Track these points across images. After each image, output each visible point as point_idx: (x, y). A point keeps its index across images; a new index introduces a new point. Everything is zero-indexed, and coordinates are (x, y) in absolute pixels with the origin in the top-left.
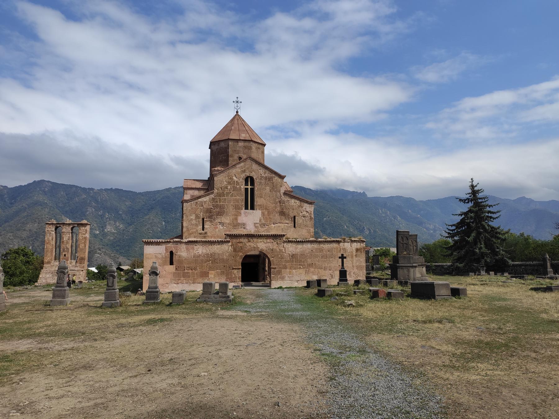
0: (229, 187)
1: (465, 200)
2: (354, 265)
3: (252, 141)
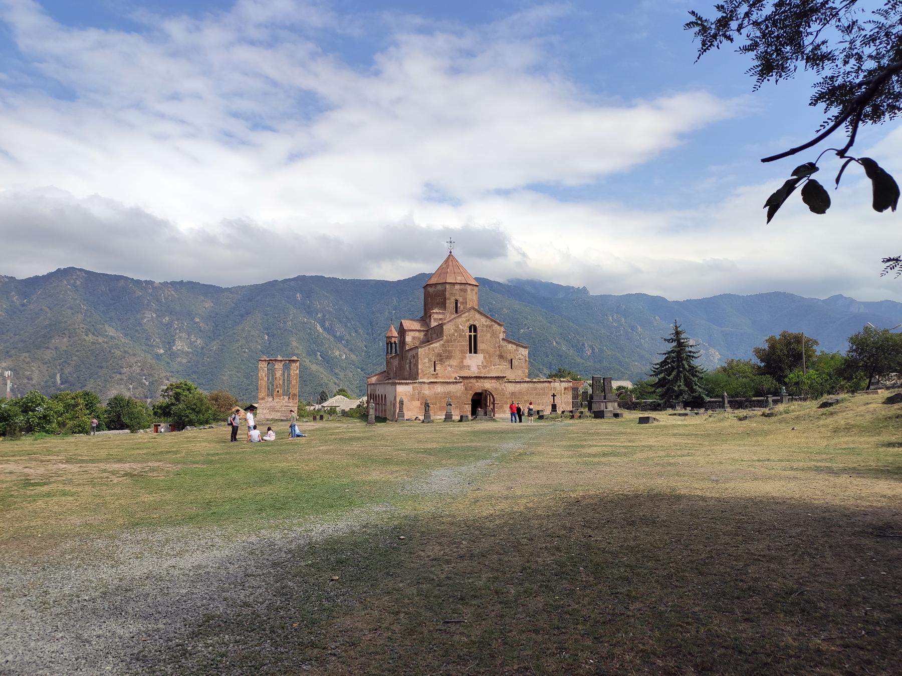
0: (456, 335)
1: (670, 340)
2: (563, 401)
3: (468, 284)
